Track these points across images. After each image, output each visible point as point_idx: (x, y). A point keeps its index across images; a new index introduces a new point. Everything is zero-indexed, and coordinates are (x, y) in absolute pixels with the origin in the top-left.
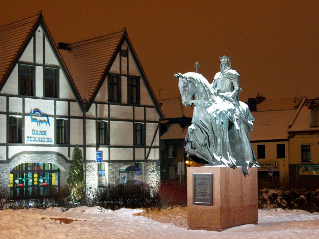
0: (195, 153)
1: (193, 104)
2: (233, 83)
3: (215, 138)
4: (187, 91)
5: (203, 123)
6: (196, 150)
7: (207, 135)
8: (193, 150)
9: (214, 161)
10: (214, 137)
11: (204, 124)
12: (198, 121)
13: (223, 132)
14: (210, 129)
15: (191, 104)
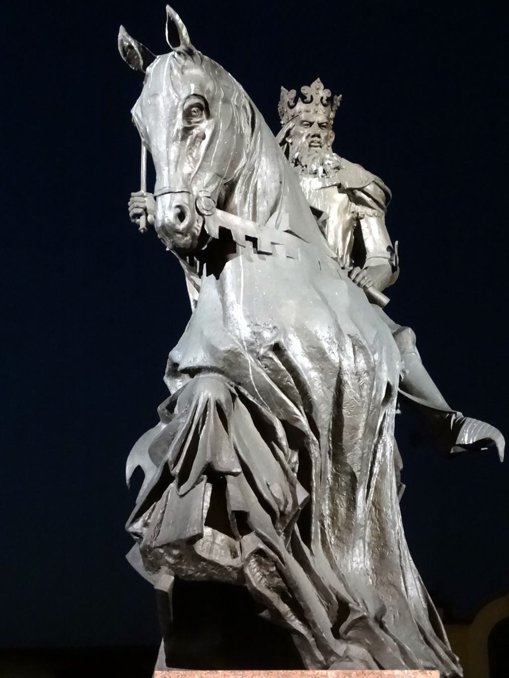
0: (237, 563)
1: (225, 233)
2: (362, 222)
3: (344, 480)
4: (205, 143)
5: (288, 363)
6: (250, 542)
7: (295, 458)
8: (221, 537)
9: (347, 640)
10: (336, 477)
11: (292, 370)
12: (251, 352)
13: (384, 455)
14: (324, 417)
15: (215, 233)
